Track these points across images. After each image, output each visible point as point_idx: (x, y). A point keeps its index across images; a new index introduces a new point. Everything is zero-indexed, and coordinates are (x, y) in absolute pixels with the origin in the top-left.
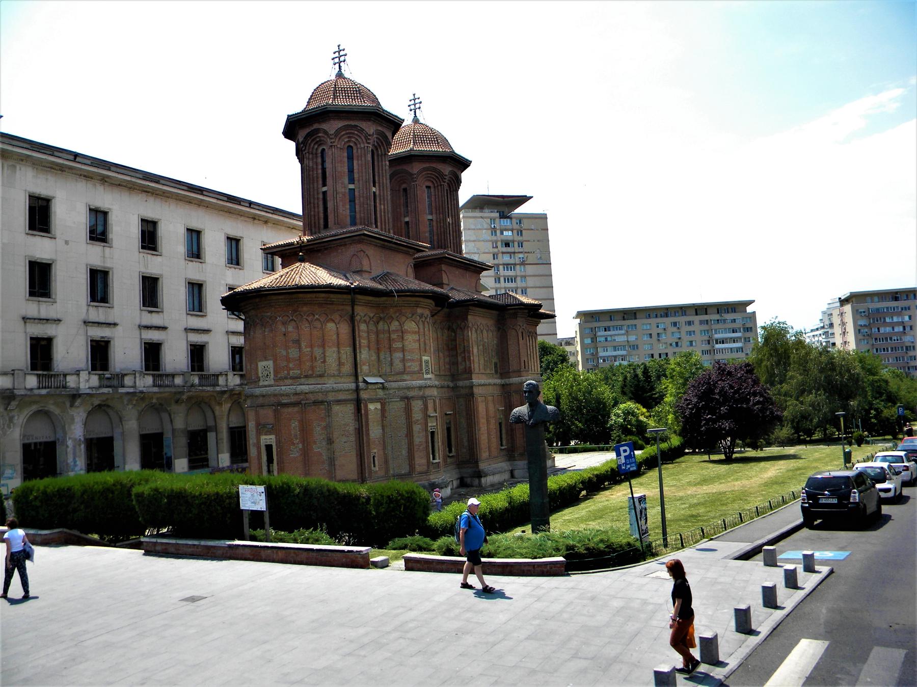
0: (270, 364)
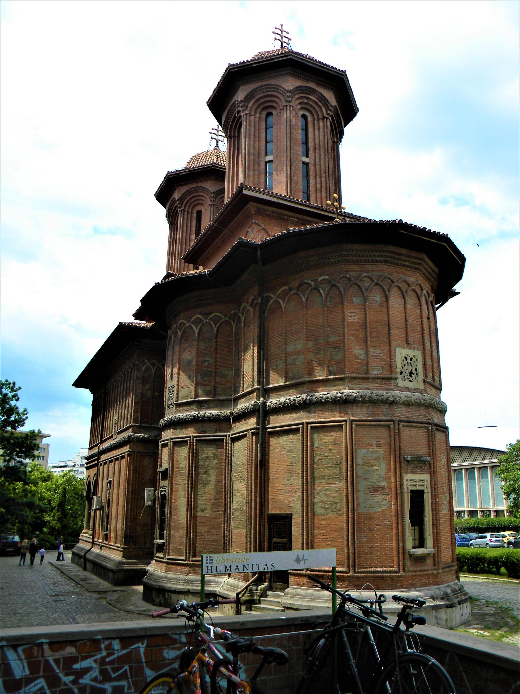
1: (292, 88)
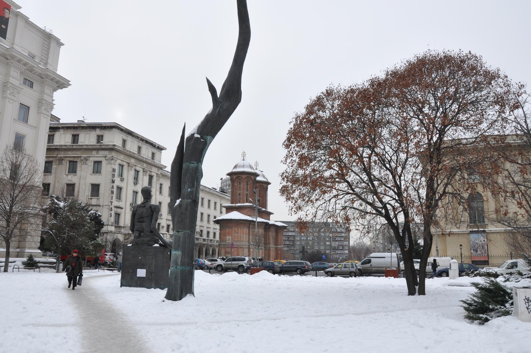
0: (230, 237)
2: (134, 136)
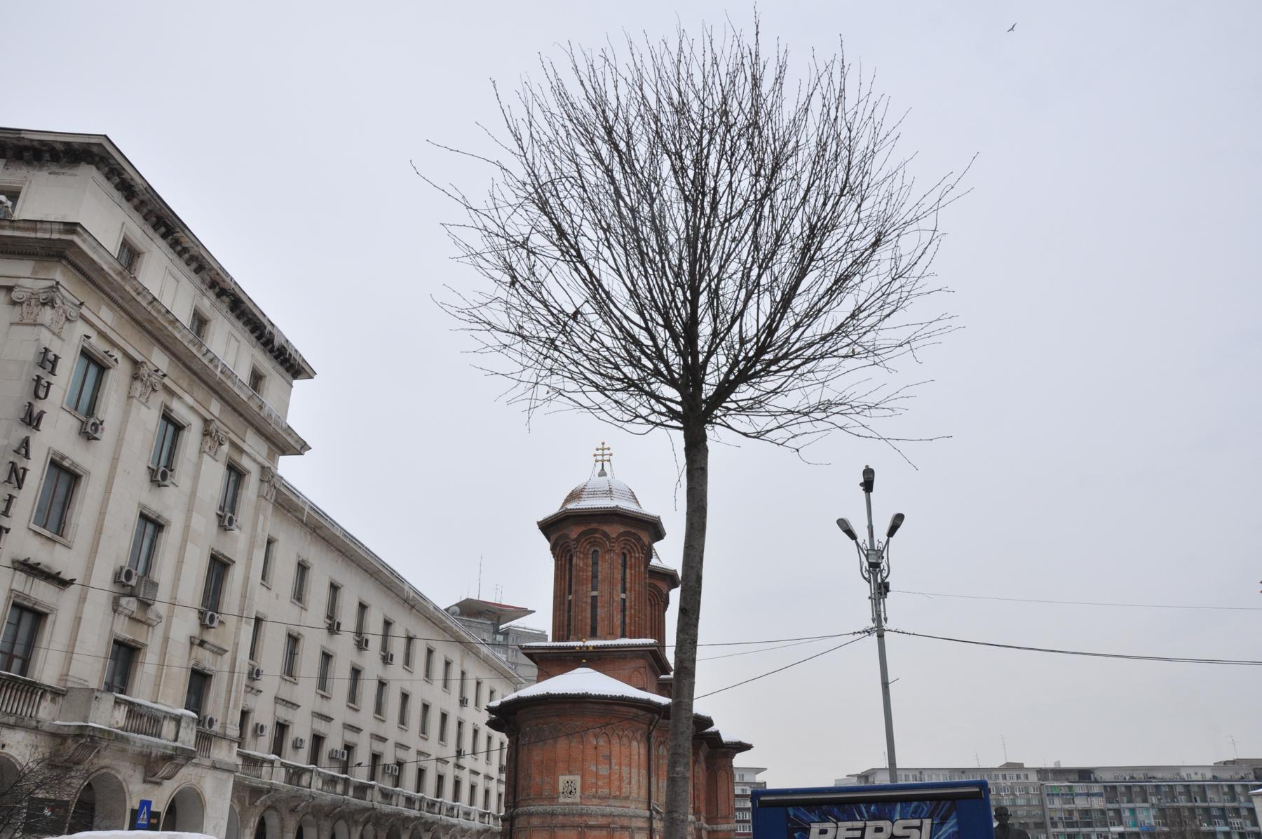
0: (577, 779)
1: (575, 536)
2: (185, 250)
